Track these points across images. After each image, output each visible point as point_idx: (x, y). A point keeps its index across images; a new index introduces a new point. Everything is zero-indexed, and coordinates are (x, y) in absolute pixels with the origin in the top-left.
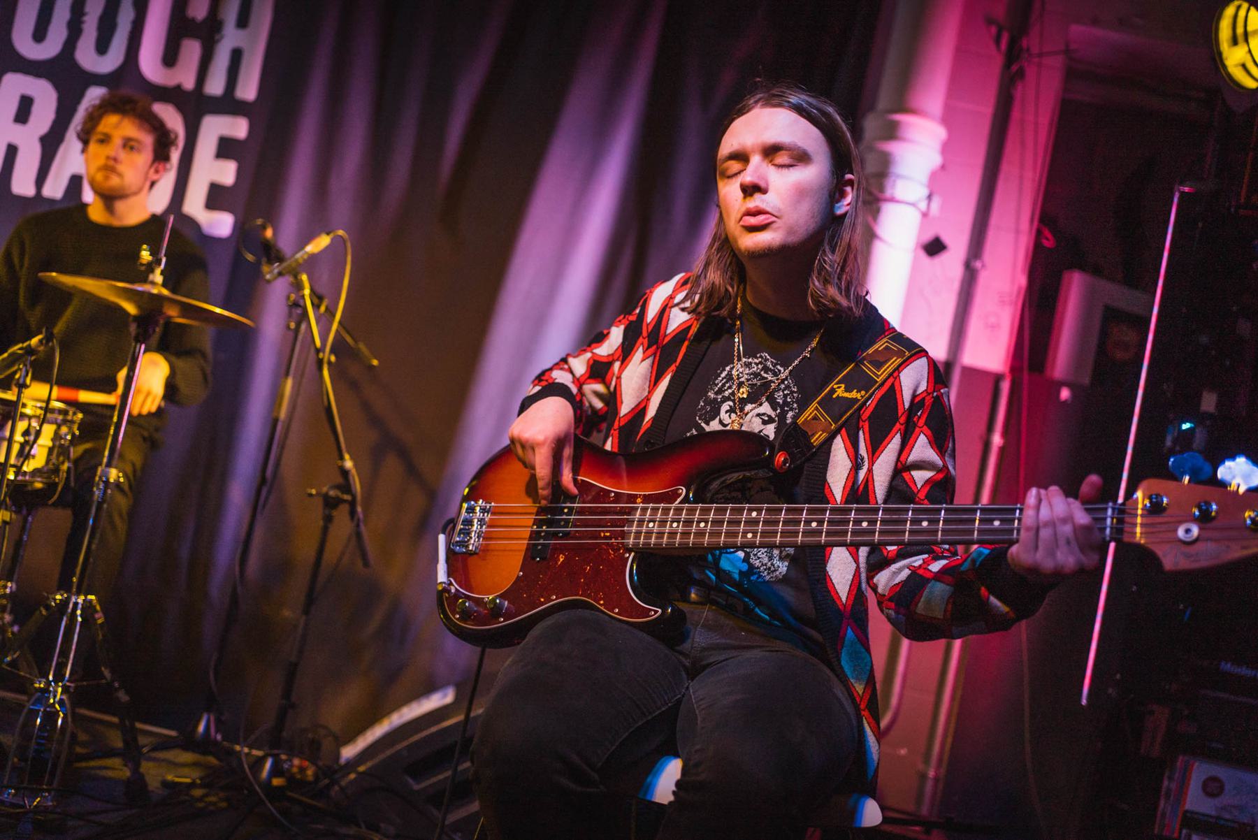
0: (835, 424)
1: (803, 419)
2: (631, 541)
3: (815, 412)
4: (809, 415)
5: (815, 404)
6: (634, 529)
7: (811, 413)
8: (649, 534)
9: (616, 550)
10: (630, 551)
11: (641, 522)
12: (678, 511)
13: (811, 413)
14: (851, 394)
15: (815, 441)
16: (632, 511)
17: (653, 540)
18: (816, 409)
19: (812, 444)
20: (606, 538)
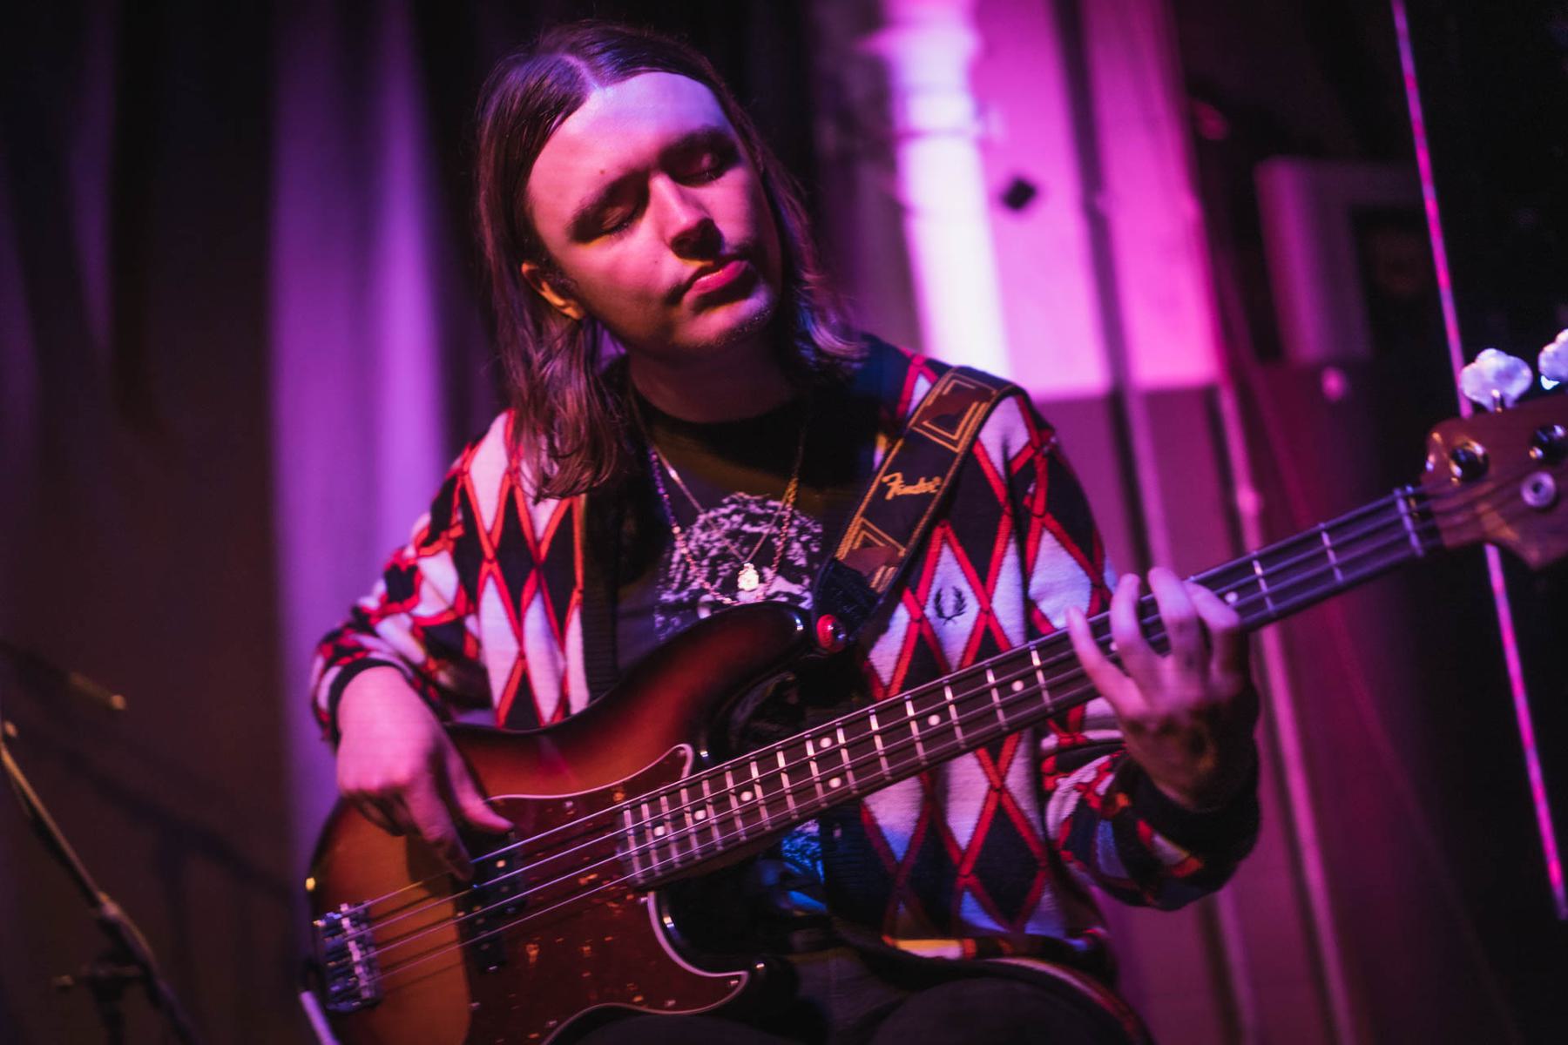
0: (905, 546)
1: (846, 551)
2: (638, 872)
3: (864, 533)
5: (858, 520)
6: (633, 849)
8: (663, 847)
9: (618, 896)
10: (643, 891)
11: (640, 834)
12: (694, 788)
13: (857, 536)
16: (615, 820)
17: (675, 856)
18: (864, 527)
19: (873, 590)
20: (592, 884)
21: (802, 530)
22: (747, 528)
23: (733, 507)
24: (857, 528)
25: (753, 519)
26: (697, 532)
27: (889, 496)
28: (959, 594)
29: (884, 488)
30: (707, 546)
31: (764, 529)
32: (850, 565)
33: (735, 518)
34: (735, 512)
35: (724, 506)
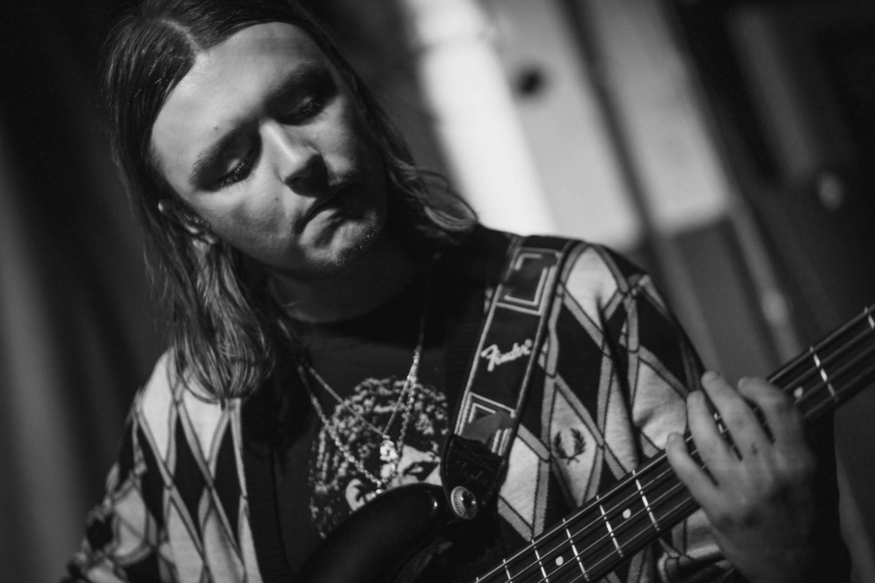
0: (514, 407)
1: (462, 426)
3: (475, 405)
4: (468, 415)
5: (468, 395)
7: (469, 411)
13: (469, 411)
14: (513, 352)
15: (498, 449)
18: (474, 400)
19: (496, 454)
21: (427, 401)
22: (378, 409)
23: (364, 393)
24: (468, 402)
25: (383, 401)
26: (336, 421)
27: (491, 368)
28: (577, 435)
29: (484, 362)
30: (347, 433)
31: (393, 408)
32: (468, 438)
33: (368, 403)
34: (368, 397)
35: (358, 394)
